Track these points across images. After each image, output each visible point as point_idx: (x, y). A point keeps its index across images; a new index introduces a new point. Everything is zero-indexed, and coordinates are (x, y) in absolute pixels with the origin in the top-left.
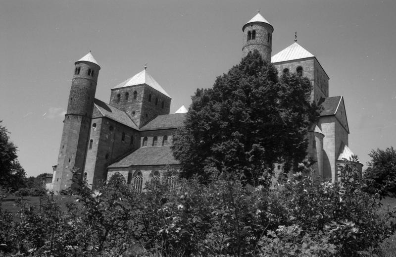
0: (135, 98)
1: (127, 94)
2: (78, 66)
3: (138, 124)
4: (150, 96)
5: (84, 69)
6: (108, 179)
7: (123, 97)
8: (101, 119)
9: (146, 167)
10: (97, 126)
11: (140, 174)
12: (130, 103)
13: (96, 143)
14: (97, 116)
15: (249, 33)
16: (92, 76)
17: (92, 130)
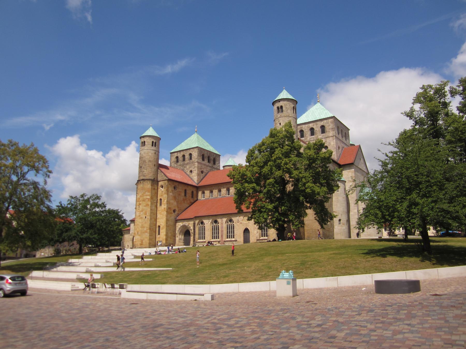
0: (191, 158)
1: (184, 156)
2: (143, 140)
3: (196, 182)
4: (203, 155)
5: (149, 141)
6: (177, 229)
7: (181, 158)
8: (166, 181)
9: (208, 217)
10: (164, 188)
11: (202, 223)
12: (187, 164)
13: (164, 202)
15: (278, 108)
16: (155, 146)
17: (159, 190)
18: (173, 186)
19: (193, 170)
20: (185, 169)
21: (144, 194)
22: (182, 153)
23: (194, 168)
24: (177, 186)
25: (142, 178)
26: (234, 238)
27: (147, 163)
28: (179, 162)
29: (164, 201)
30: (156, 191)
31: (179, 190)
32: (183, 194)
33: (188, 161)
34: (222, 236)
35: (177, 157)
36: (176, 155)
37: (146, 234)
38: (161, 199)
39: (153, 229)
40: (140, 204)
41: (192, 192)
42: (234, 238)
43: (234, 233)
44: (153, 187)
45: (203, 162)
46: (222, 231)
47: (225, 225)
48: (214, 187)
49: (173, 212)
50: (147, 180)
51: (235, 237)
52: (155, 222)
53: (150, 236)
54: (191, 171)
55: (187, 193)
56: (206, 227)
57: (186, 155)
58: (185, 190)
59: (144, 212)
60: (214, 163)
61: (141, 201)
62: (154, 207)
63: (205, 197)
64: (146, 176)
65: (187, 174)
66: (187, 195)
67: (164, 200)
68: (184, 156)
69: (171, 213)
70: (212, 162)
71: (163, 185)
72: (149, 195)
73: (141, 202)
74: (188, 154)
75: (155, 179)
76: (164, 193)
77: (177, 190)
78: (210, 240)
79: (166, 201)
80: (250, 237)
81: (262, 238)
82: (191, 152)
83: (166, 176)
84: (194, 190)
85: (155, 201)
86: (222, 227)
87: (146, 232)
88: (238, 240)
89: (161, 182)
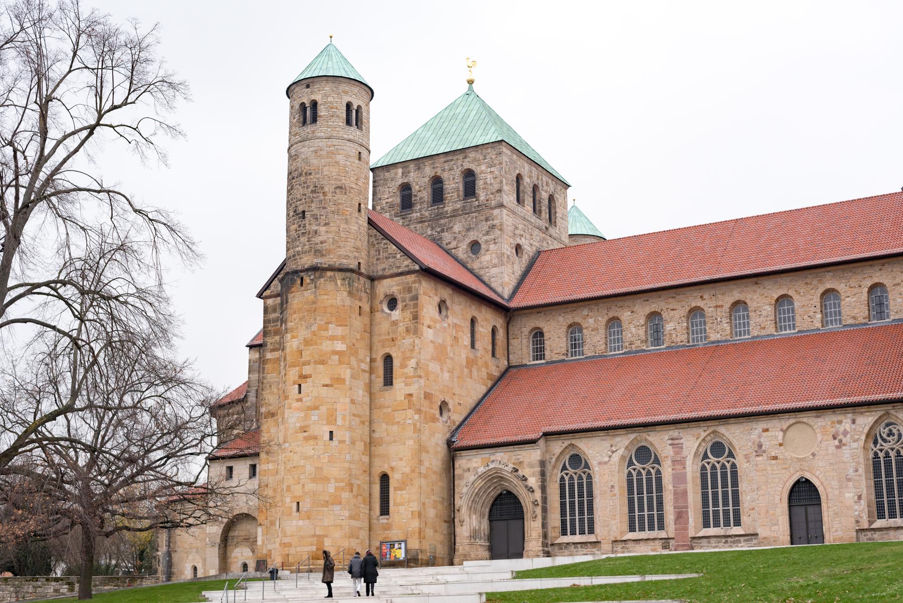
1: (437, 183)
8: (411, 278)
10: (400, 305)
12: (455, 214)
14: (395, 271)
17: (378, 315)
18: (437, 300)
19: (482, 240)
20: (447, 237)
21: (323, 333)
22: (429, 171)
23: (487, 233)
24: (448, 303)
25: (307, 261)
26: (738, 523)
27: (329, 196)
28: (418, 207)
29: (403, 366)
30: (366, 320)
31: (456, 321)
33: (459, 205)
34: (681, 516)
35: (406, 188)
36: (399, 177)
38: (388, 359)
40: (304, 377)
41: (494, 331)
42: (738, 523)
43: (736, 502)
44: (358, 303)
45: (519, 209)
46: (681, 495)
47: (692, 469)
48: (585, 312)
49: (438, 412)
50: (331, 269)
51: (744, 519)
54: (475, 246)
55: (477, 336)
56: (596, 480)
57: (445, 176)
58: (473, 321)
60: (551, 220)
61: (307, 363)
63: (547, 353)
64: (329, 252)
65: (456, 259)
66: (478, 345)
67: (406, 359)
68: (437, 183)
70: (545, 215)
71: (399, 297)
72: (343, 338)
73: (307, 370)
74: (457, 172)
76: (401, 328)
77: (452, 320)
78: (622, 533)
79: (412, 363)
80: (825, 519)
81: (879, 523)
82: (472, 167)
83: (407, 254)
84: (499, 322)
86: (679, 478)
88: (762, 532)
89: (386, 282)
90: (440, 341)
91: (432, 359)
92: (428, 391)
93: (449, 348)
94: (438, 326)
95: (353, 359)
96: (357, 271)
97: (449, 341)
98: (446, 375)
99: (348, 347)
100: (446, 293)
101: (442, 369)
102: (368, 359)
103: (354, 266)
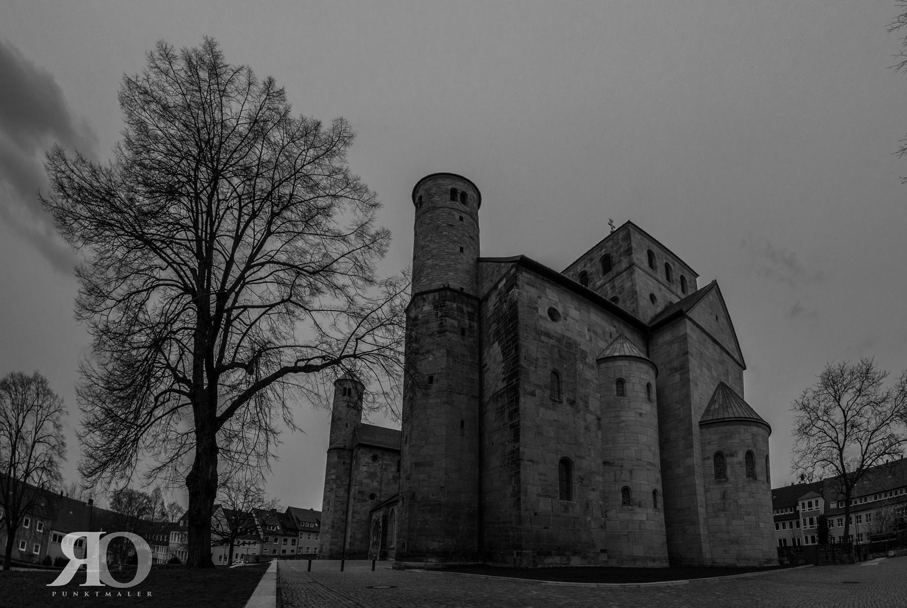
24: (379, 456)
31: (385, 462)
32: (394, 469)
37: (327, 535)
39: (338, 527)
44: (343, 460)
52: (345, 517)
53: (332, 538)
59: (327, 500)
62: (342, 493)
69: (365, 501)
72: (334, 474)
75: (347, 447)
77: (380, 462)
85: (344, 483)
87: (328, 532)
90: (372, 471)
91: (366, 478)
92: (361, 490)
93: (378, 473)
94: (370, 465)
95: (338, 482)
96: (344, 449)
97: (378, 470)
98: (375, 484)
99: (337, 477)
100: (378, 453)
101: (372, 482)
102: (348, 480)
103: (342, 446)
